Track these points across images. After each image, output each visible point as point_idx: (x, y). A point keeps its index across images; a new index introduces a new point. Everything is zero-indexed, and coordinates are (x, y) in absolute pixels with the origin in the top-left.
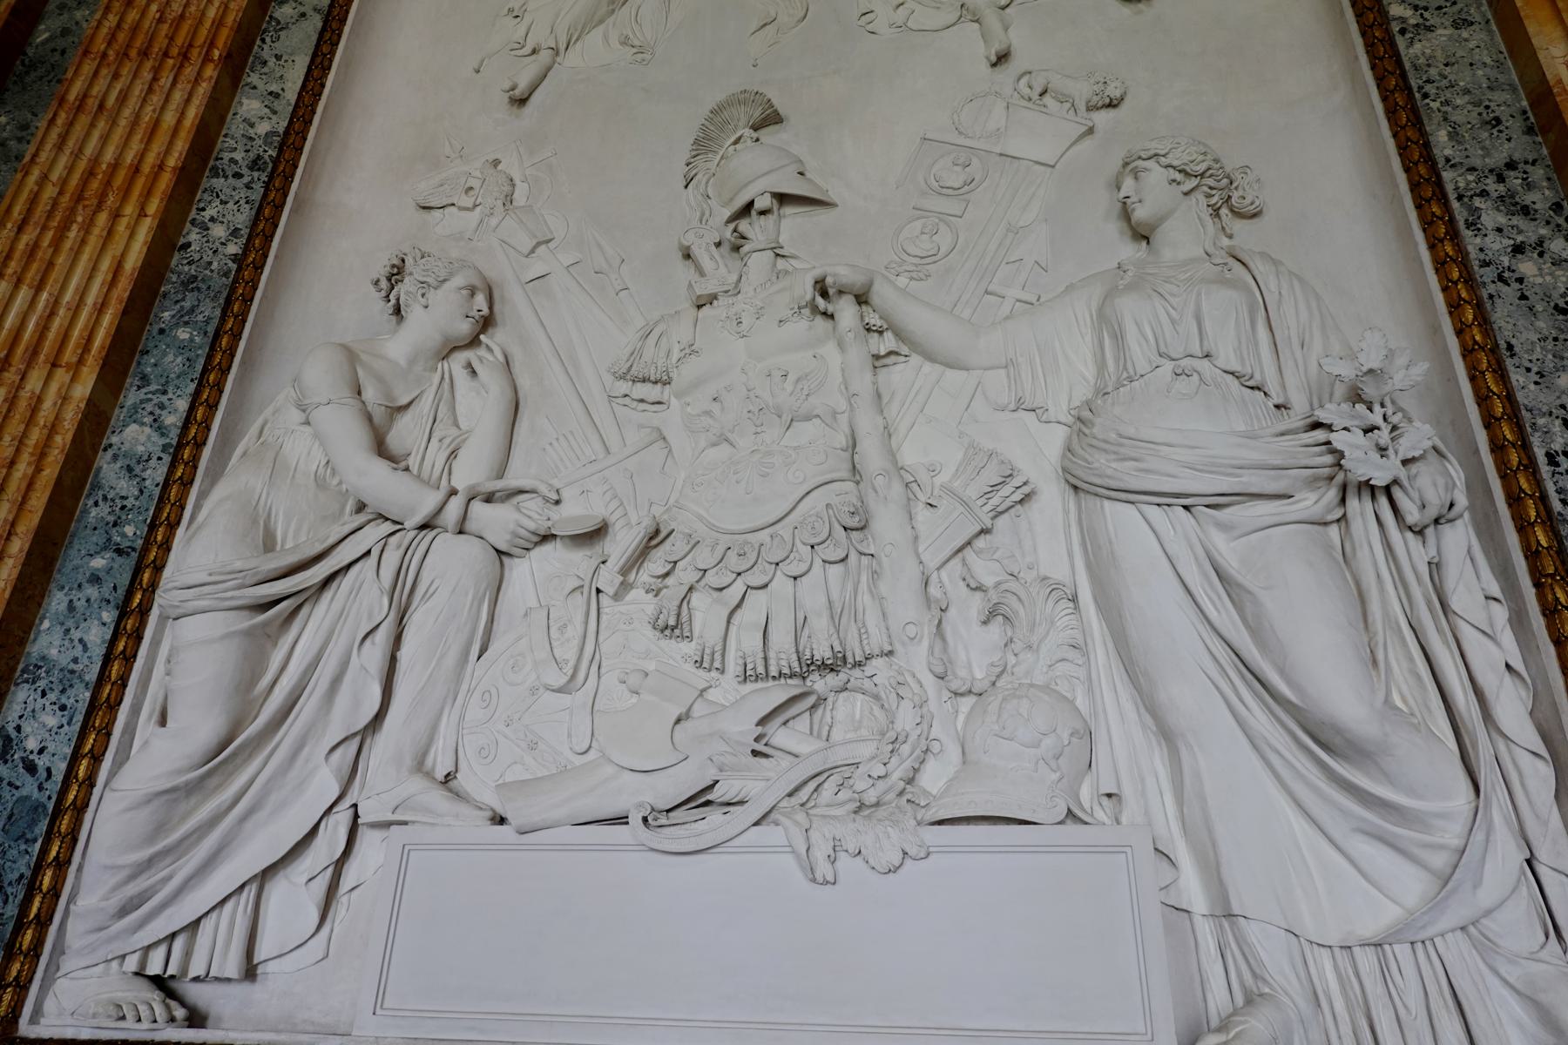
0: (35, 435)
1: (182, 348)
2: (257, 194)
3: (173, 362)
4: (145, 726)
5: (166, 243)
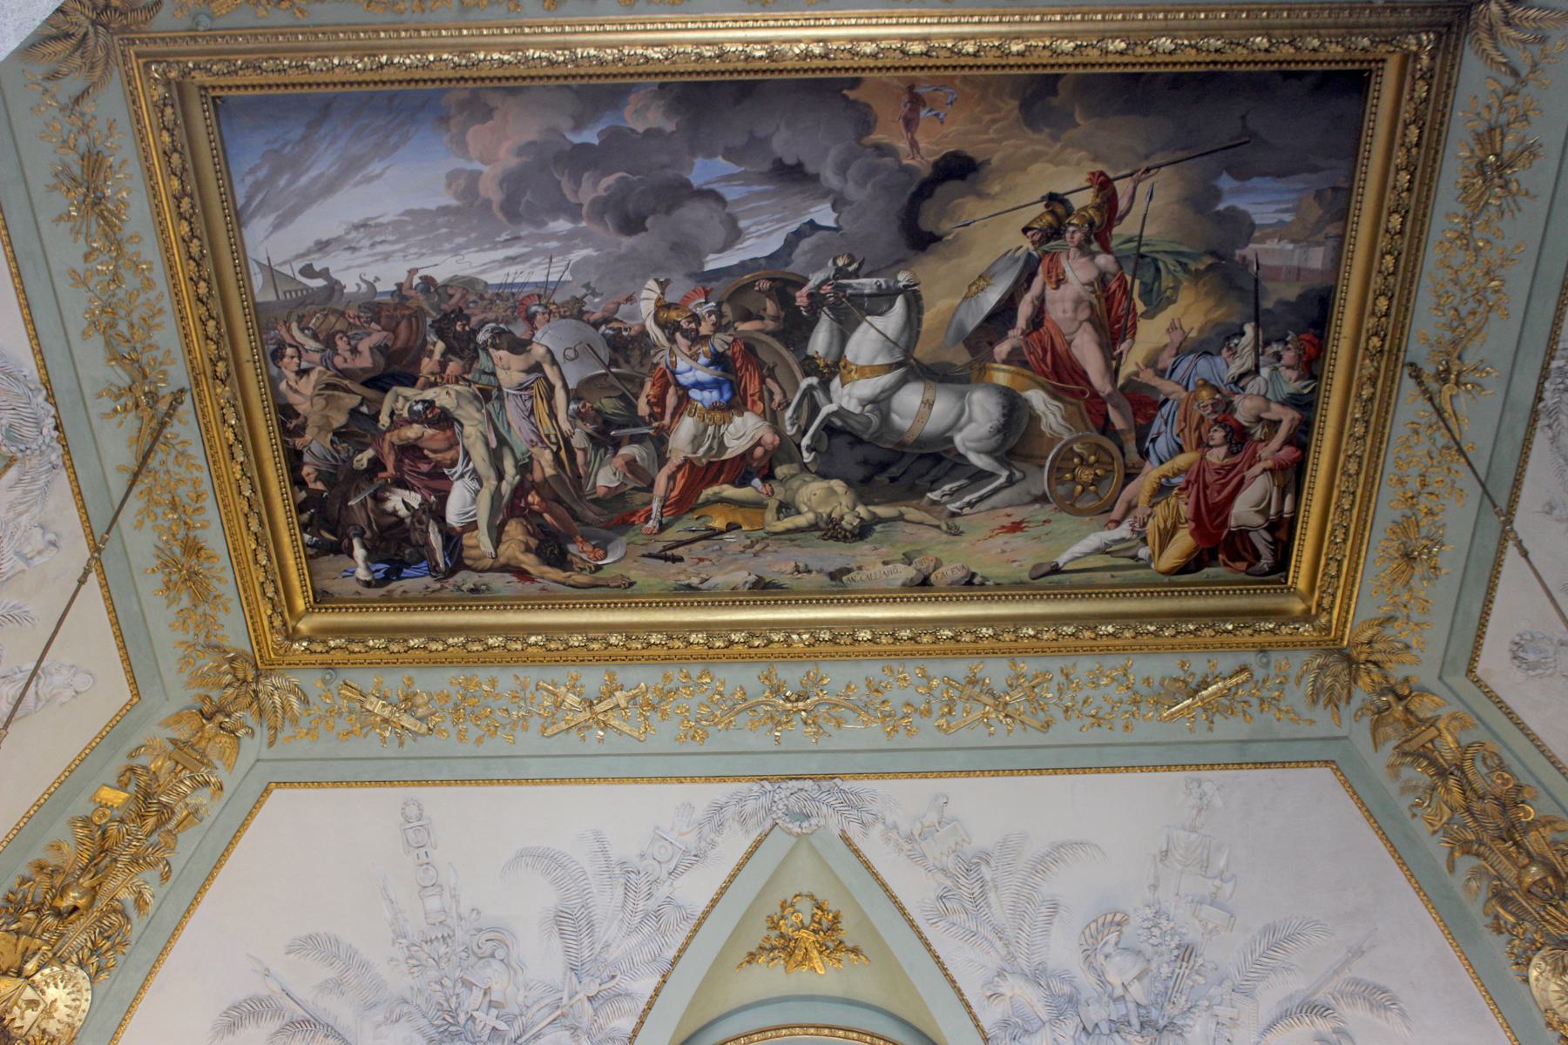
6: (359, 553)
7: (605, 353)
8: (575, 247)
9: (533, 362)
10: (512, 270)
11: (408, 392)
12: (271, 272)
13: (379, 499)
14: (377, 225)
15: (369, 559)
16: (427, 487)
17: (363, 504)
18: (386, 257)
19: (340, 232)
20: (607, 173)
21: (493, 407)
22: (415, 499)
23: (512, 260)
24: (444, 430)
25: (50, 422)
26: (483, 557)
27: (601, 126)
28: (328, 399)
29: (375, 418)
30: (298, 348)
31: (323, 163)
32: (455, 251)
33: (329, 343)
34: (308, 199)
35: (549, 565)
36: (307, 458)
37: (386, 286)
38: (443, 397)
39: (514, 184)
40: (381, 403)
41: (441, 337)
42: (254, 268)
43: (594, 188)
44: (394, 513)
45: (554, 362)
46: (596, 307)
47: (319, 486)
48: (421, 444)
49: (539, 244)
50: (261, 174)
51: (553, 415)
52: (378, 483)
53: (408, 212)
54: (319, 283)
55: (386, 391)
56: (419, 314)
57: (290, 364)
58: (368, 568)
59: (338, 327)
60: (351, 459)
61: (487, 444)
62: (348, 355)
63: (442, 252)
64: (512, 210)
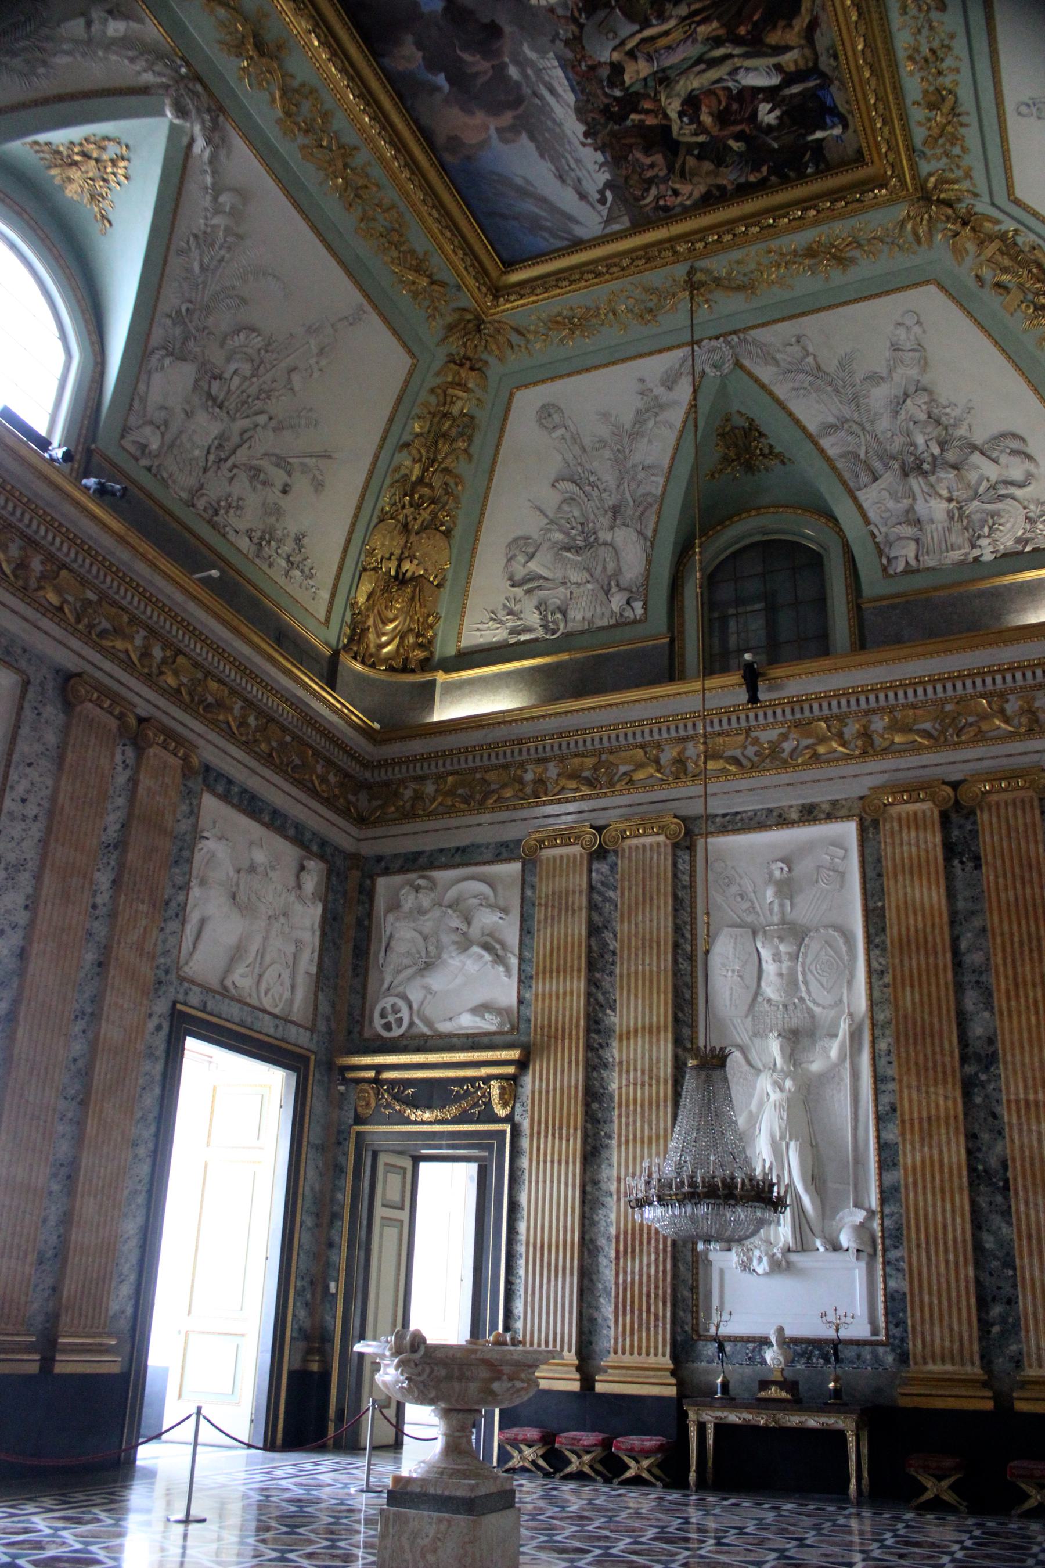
6: (819, 135)
7: (601, 14)
8: (527, 59)
9: (627, 58)
10: (560, 90)
11: (675, 128)
12: (608, 221)
13: (770, 128)
14: (557, 169)
15: (824, 128)
16: (752, 101)
17: (775, 139)
18: (578, 161)
19: (570, 190)
20: (460, 60)
21: (672, 74)
22: (764, 108)
23: (552, 91)
24: (700, 101)
25: (714, 343)
26: (803, 56)
27: (430, 76)
28: (693, 174)
29: (701, 145)
30: (657, 198)
31: (530, 207)
32: (560, 125)
33: (650, 182)
34: (553, 209)
35: (799, 8)
36: (742, 180)
37: (599, 157)
38: (673, 108)
39: (495, 109)
40: (688, 144)
41: (625, 117)
42: (608, 230)
43: (476, 63)
44: (778, 118)
45: (622, 43)
46: (566, 31)
47: (765, 169)
48: (715, 110)
49: (534, 79)
50: (546, 235)
51: (666, 33)
52: (755, 132)
53: (542, 156)
54: (609, 194)
55: (677, 143)
56: (613, 134)
57: (671, 201)
58: (832, 128)
59: (636, 177)
60: (737, 153)
61: (704, 71)
62: (656, 170)
63: (563, 131)
64: (518, 101)
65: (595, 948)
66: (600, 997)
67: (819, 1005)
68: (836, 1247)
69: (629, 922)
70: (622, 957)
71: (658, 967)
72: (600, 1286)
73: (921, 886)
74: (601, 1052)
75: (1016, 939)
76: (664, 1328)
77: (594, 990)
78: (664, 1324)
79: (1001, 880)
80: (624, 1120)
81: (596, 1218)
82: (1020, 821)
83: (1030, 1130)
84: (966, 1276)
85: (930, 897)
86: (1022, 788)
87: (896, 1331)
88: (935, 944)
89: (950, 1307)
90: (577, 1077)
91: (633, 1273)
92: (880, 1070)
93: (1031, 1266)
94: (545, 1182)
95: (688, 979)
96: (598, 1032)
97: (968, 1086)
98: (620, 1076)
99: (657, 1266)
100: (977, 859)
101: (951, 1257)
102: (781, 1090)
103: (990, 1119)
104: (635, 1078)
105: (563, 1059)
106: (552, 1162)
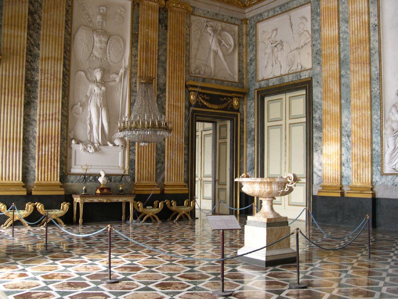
0: (366, 118)
1: (377, 105)
2: (379, 83)
3: (377, 107)
4: (386, 147)
5: (371, 92)
65: (30, 20)
66: (32, 42)
67: (112, 62)
68: (115, 145)
69: (48, 14)
70: (44, 27)
71: (59, 35)
72: (30, 155)
73: (151, 31)
74: (32, 63)
75: (176, 55)
76: (57, 171)
77: (30, 38)
78: (57, 169)
79: (174, 36)
80: (42, 92)
81: (28, 129)
82: (181, 19)
83: (173, 114)
84: (154, 156)
85: (154, 35)
86: (183, 9)
87: (132, 172)
88: (153, 51)
89: (149, 164)
90: (22, 72)
91: (45, 151)
92: (132, 88)
93: (170, 153)
94: (7, 113)
95: (68, 42)
96: (31, 55)
97: (158, 97)
98: (41, 75)
99: (55, 149)
100: (166, 26)
101: (150, 149)
102: (101, 89)
103: (162, 109)
104: (48, 77)
105: (16, 64)
106: (11, 106)
